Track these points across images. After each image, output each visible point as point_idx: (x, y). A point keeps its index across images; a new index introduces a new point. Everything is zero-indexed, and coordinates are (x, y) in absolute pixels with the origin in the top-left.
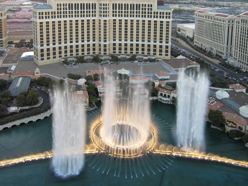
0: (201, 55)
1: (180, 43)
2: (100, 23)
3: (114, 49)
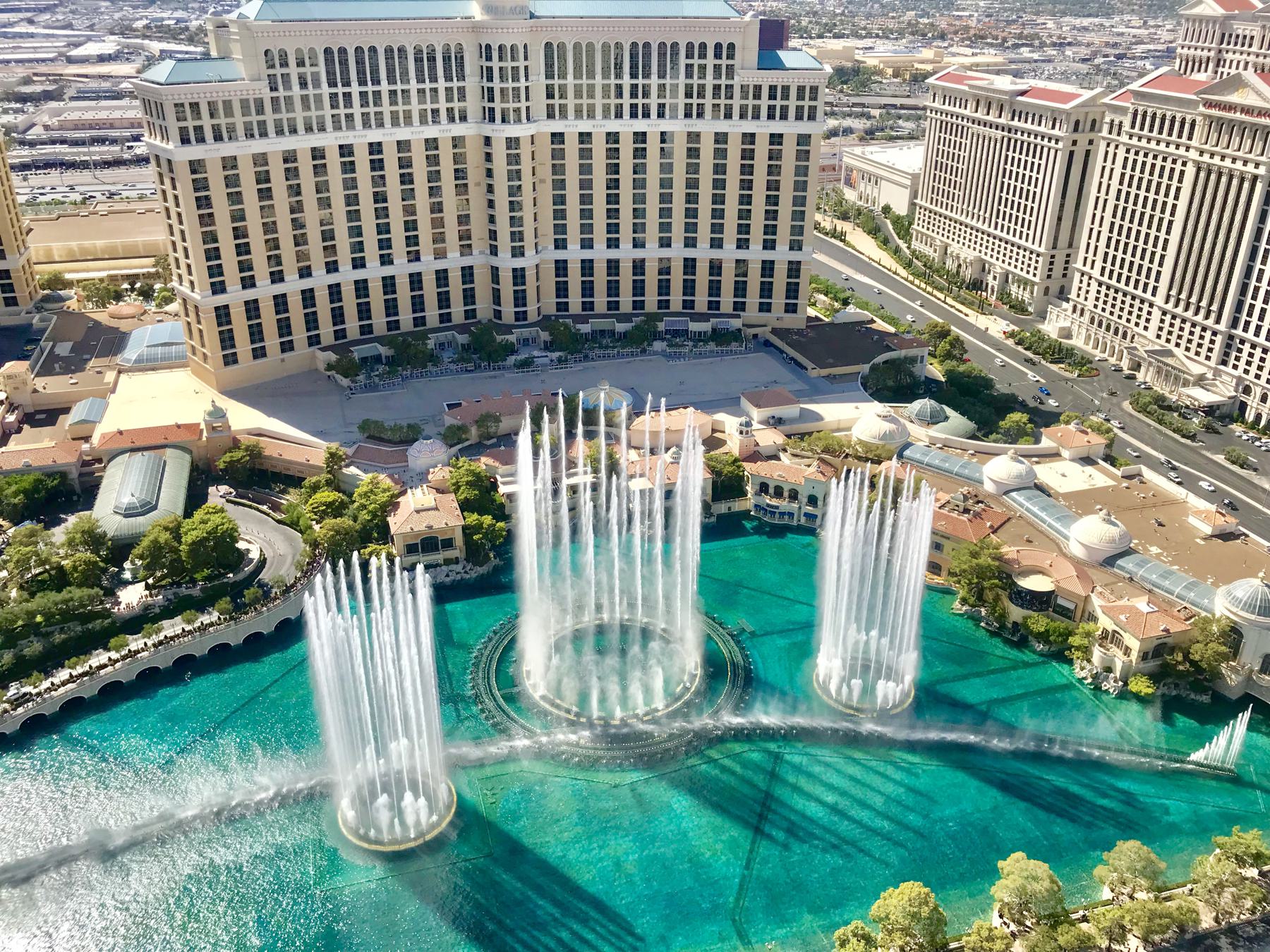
0: (953, 310)
1: (852, 243)
2: (488, 157)
3: (562, 290)
